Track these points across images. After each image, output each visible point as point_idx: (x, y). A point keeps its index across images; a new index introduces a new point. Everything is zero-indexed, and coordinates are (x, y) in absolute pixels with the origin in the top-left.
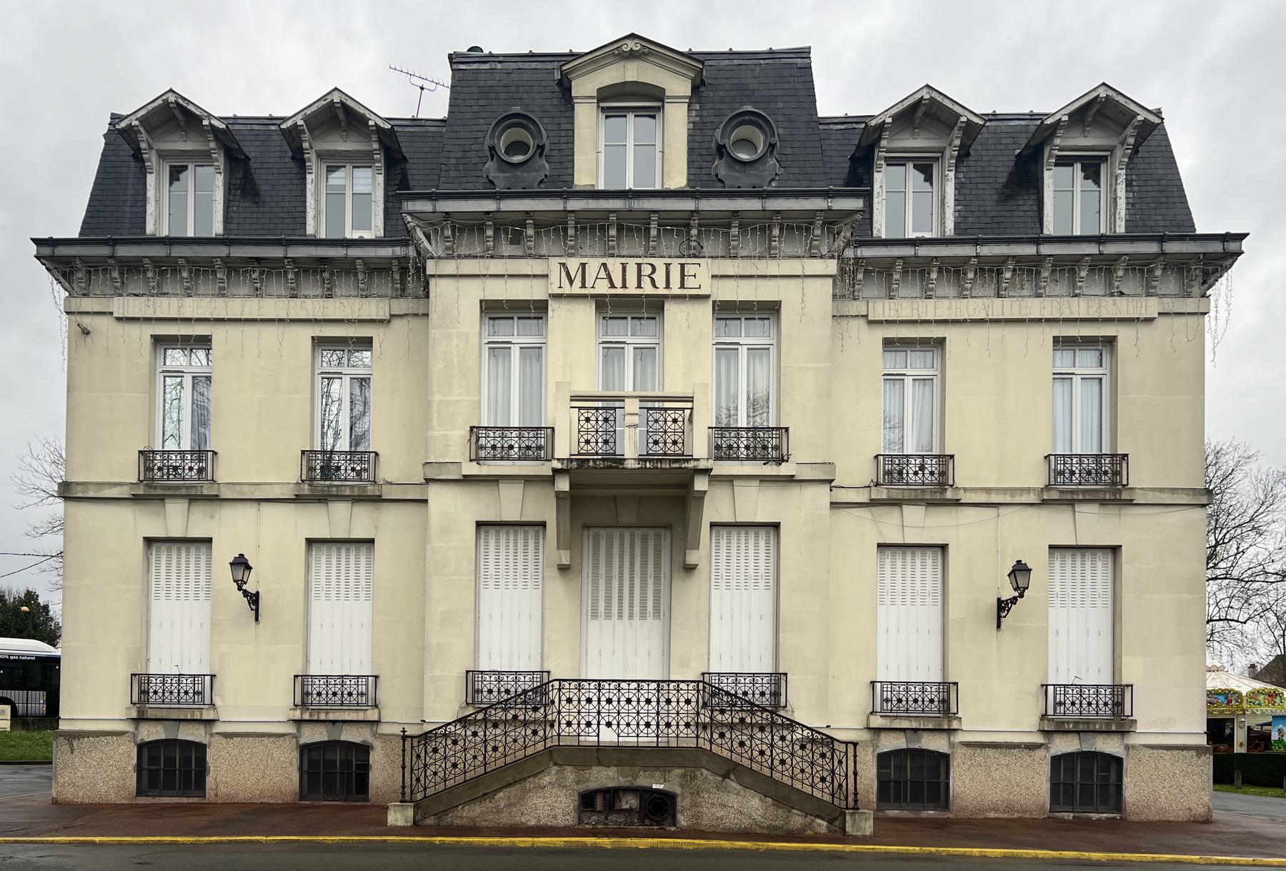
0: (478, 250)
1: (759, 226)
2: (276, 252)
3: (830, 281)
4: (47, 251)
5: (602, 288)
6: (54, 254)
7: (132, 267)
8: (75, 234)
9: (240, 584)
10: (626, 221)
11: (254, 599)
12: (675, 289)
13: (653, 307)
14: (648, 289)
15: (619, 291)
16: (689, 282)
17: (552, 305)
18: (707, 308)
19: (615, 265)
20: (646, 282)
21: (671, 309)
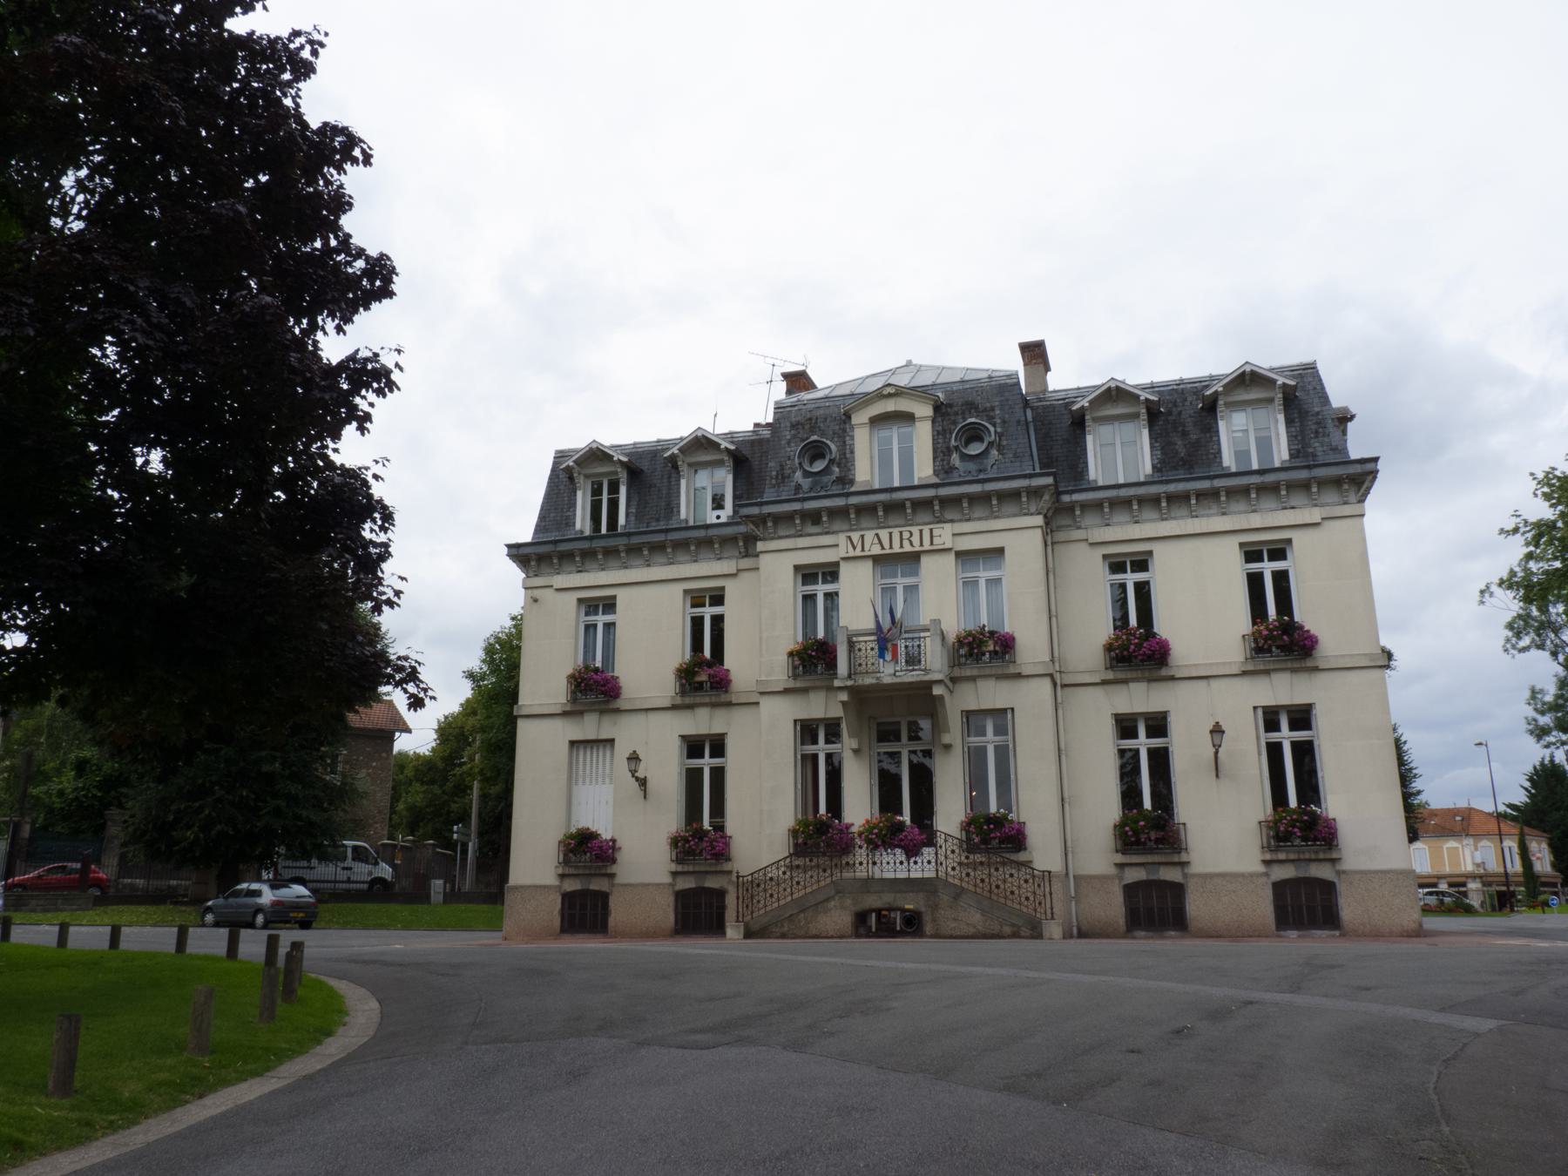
0: (792, 532)
1: (983, 499)
2: (661, 537)
3: (1039, 531)
4: (514, 551)
5: (876, 550)
6: (518, 553)
7: (566, 557)
8: (529, 539)
9: (633, 772)
10: (892, 507)
11: (643, 783)
12: (927, 546)
13: (915, 557)
14: (907, 548)
15: (888, 551)
16: (936, 540)
17: (842, 564)
18: (952, 556)
19: (884, 534)
20: (906, 543)
21: (924, 560)
